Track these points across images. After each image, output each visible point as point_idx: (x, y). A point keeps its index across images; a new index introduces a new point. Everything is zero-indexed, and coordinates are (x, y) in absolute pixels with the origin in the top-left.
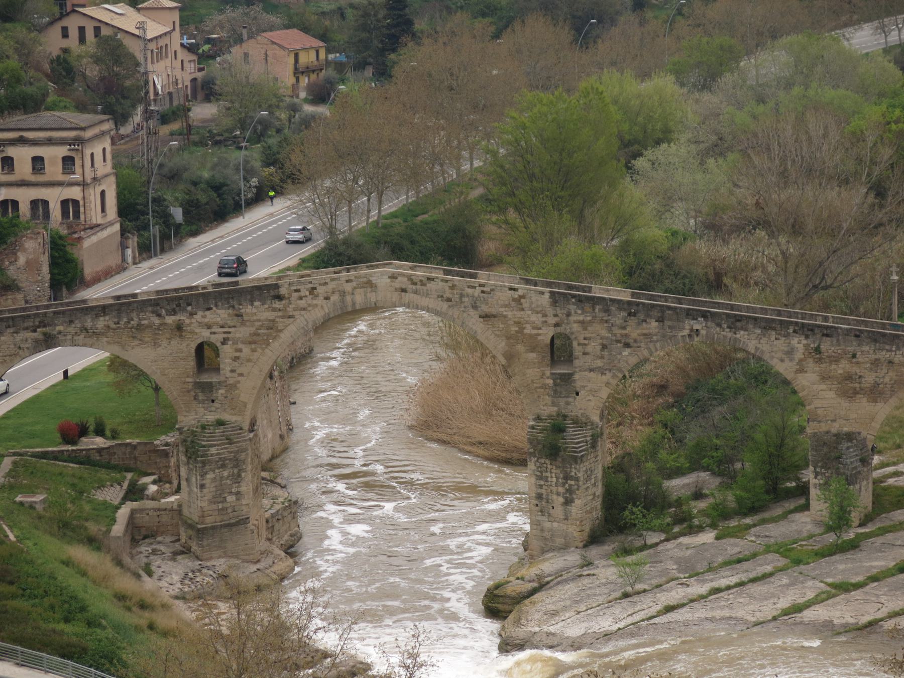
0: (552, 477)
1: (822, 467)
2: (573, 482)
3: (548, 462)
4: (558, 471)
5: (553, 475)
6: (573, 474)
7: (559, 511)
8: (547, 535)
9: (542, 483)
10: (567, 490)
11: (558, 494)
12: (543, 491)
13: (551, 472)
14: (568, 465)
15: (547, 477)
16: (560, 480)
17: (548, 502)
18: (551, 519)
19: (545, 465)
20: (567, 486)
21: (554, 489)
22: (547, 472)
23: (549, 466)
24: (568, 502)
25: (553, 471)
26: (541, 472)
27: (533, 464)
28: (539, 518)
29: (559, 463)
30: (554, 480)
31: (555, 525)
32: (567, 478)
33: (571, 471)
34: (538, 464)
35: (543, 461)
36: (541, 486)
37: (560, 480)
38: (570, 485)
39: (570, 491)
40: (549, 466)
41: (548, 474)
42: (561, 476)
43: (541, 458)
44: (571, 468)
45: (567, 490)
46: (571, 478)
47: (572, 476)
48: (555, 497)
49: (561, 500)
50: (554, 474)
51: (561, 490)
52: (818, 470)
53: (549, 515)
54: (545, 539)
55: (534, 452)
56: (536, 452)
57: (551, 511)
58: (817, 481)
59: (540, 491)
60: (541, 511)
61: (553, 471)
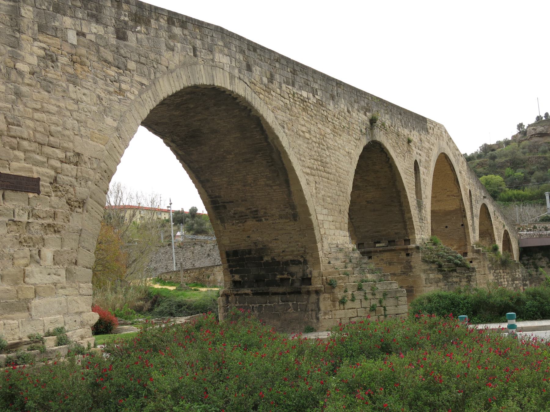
0: (504, 281)
3: (501, 271)
4: (508, 276)
5: (505, 280)
6: (517, 276)
10: (515, 288)
13: (504, 278)
14: (514, 271)
15: (502, 282)
16: (510, 282)
19: (500, 274)
22: (501, 278)
23: (502, 274)
25: (505, 277)
26: (497, 279)
27: (492, 275)
29: (508, 271)
30: (506, 283)
33: (516, 275)
34: (495, 274)
35: (498, 271)
37: (510, 282)
40: (502, 274)
41: (502, 280)
42: (510, 279)
43: (497, 270)
44: (516, 272)
47: (516, 278)
55: (492, 267)
56: (494, 266)
61: (505, 277)
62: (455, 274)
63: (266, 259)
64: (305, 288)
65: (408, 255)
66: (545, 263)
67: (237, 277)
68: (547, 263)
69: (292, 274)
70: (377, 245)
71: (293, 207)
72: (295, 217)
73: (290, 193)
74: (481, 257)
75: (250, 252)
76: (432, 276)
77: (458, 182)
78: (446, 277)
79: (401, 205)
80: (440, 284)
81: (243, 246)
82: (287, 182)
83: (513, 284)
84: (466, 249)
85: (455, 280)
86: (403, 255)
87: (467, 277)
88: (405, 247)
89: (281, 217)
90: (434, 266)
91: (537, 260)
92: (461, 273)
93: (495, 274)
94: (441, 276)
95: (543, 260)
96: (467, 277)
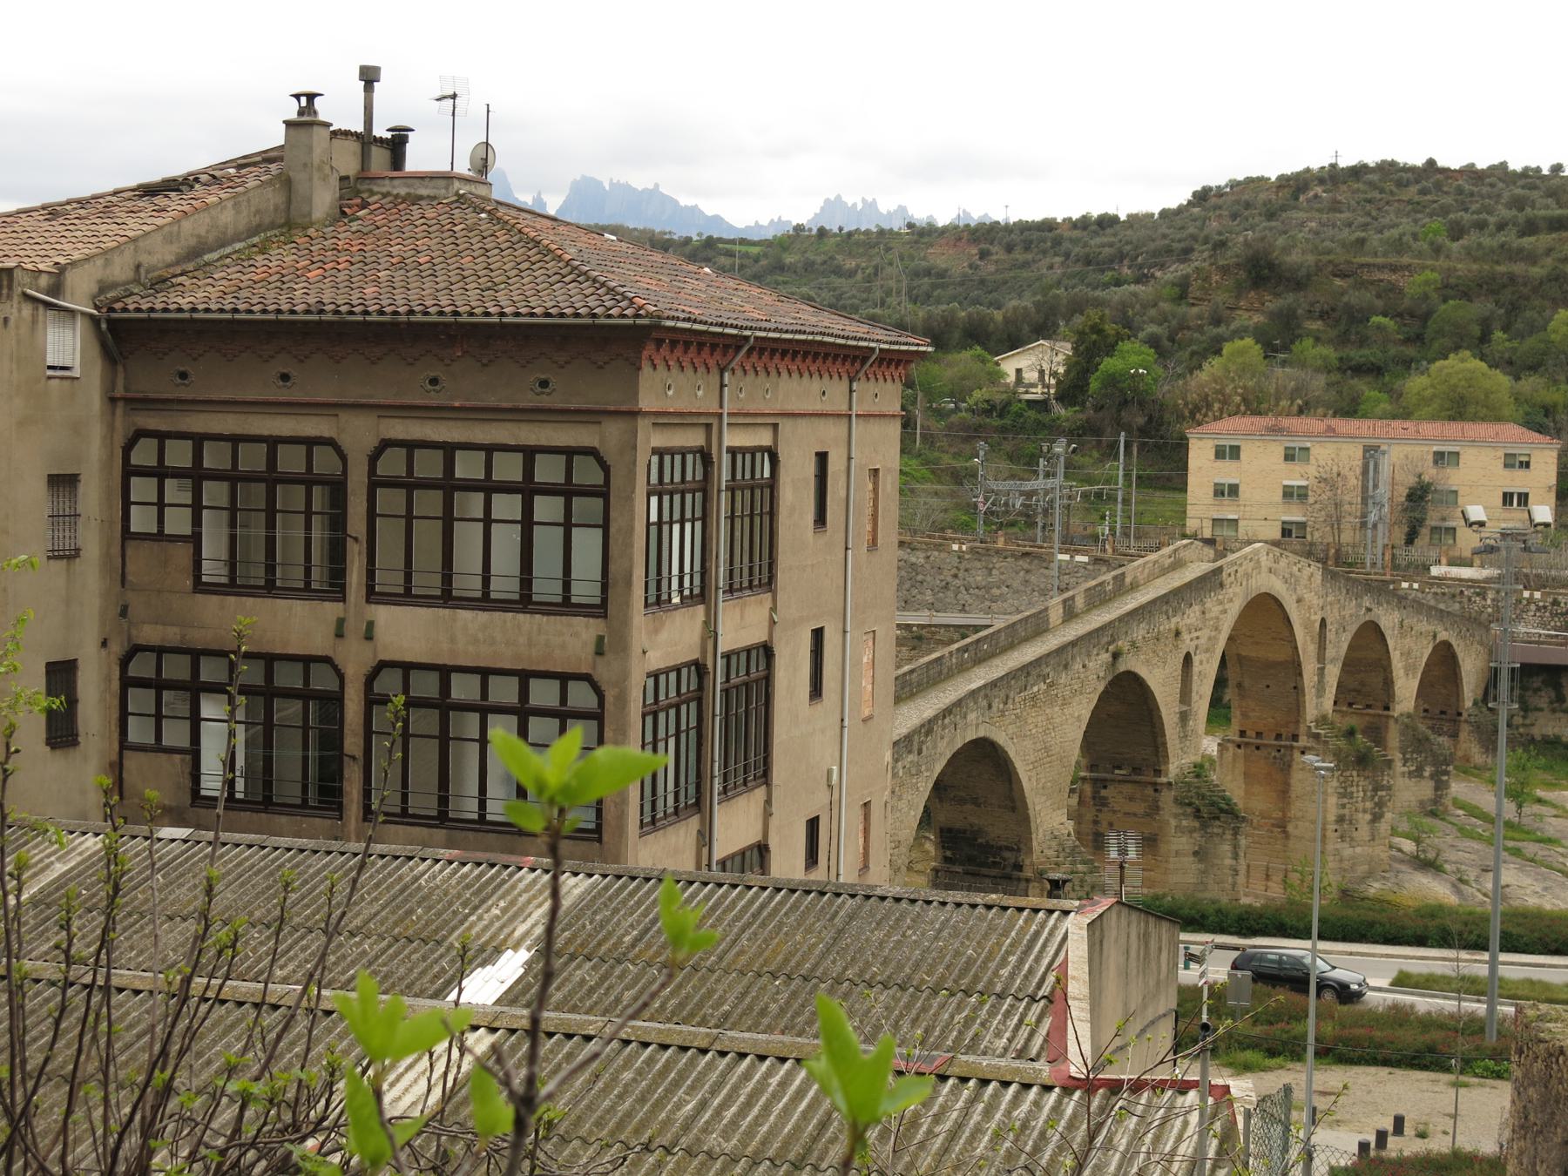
1: (1412, 752)
2: (1384, 793)
3: (1355, 773)
4: (1367, 783)
7: (1363, 832)
8: (1346, 865)
9: (1345, 801)
10: (1376, 804)
11: (1365, 811)
12: (1346, 811)
17: (1351, 823)
18: (1354, 844)
20: (1376, 799)
21: (1360, 806)
23: (1356, 779)
24: (1376, 818)
26: (1345, 788)
28: (1338, 846)
29: (1366, 773)
30: (1361, 794)
31: (1358, 850)
32: (1376, 790)
34: (1342, 779)
35: (1348, 773)
36: (1343, 806)
38: (1381, 797)
39: (1380, 804)
40: (1356, 779)
41: (1354, 789)
45: (1376, 804)
46: (1382, 788)
48: (1360, 815)
49: (1368, 817)
50: (1360, 786)
51: (1369, 805)
52: (1408, 756)
53: (1352, 839)
54: (1345, 870)
57: (1355, 834)
58: (1406, 769)
59: (1342, 812)
60: (1342, 837)
62: (1217, 823)
63: (980, 840)
64: (1016, 874)
65: (1156, 790)
66: (1547, 700)
67: (948, 853)
68: (1551, 702)
69: (1005, 860)
70: (1117, 772)
71: (1013, 800)
72: (1013, 809)
73: (1011, 790)
74: (1320, 747)
75: (965, 832)
76: (1184, 823)
77: (1289, 621)
78: (1204, 826)
79: (1153, 726)
80: (1195, 835)
81: (958, 825)
82: (1010, 781)
83: (1373, 797)
84: (1298, 728)
85: (1215, 830)
86: (1149, 791)
87: (1233, 829)
88: (1154, 779)
89: (999, 807)
90: (1189, 810)
91: (1529, 693)
92: (1225, 822)
93: (1342, 779)
94: (1197, 824)
95: (1543, 693)
96: (1233, 829)
